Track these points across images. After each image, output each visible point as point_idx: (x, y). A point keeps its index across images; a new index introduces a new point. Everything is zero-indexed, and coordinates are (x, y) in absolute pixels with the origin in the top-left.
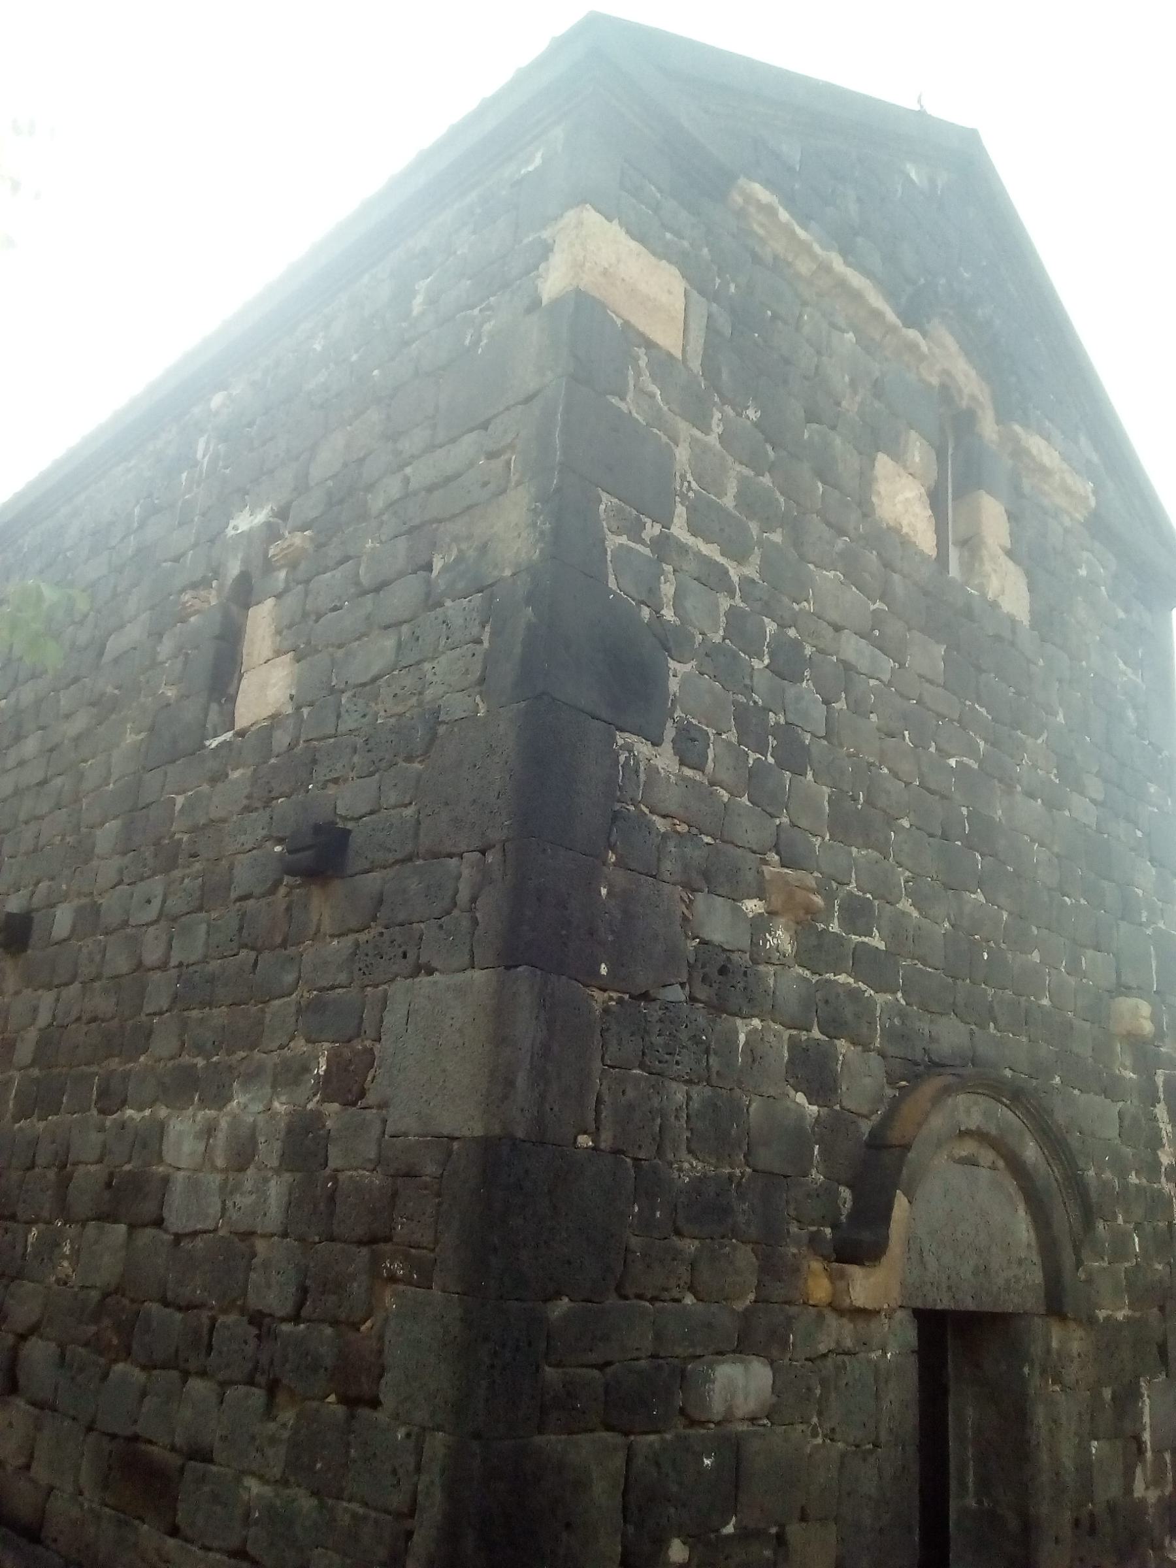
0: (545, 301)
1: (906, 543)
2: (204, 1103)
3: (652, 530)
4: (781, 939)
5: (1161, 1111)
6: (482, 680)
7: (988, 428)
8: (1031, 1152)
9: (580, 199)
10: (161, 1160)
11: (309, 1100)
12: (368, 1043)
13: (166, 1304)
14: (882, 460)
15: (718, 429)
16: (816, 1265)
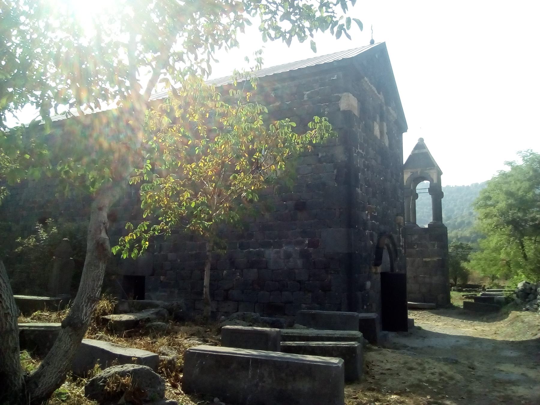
0: (341, 109)
1: (377, 138)
2: (274, 248)
3: (357, 151)
4: (369, 217)
5: (401, 236)
6: (336, 179)
7: (385, 108)
8: (391, 246)
9: (346, 90)
10: (264, 257)
11: (305, 247)
12: (318, 239)
13: (273, 281)
14: (375, 122)
15: (361, 128)
16: (373, 267)
